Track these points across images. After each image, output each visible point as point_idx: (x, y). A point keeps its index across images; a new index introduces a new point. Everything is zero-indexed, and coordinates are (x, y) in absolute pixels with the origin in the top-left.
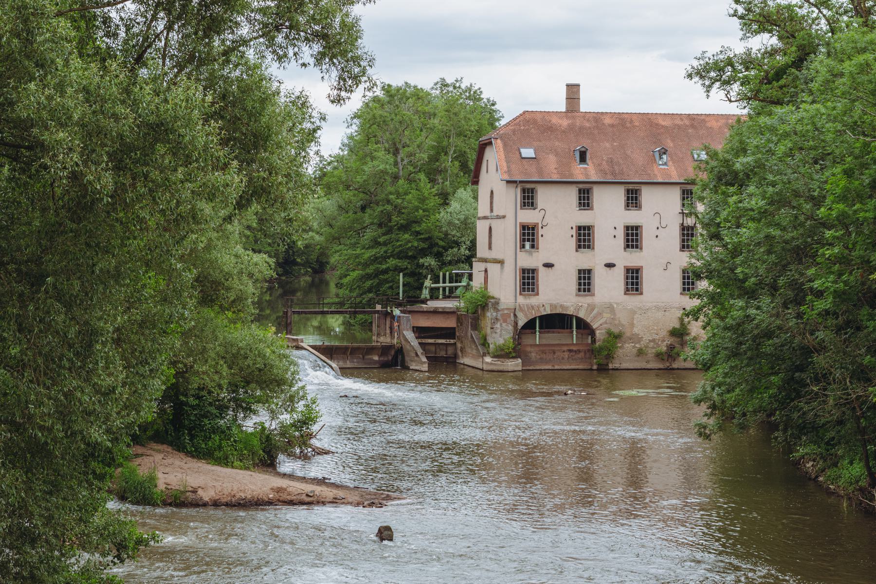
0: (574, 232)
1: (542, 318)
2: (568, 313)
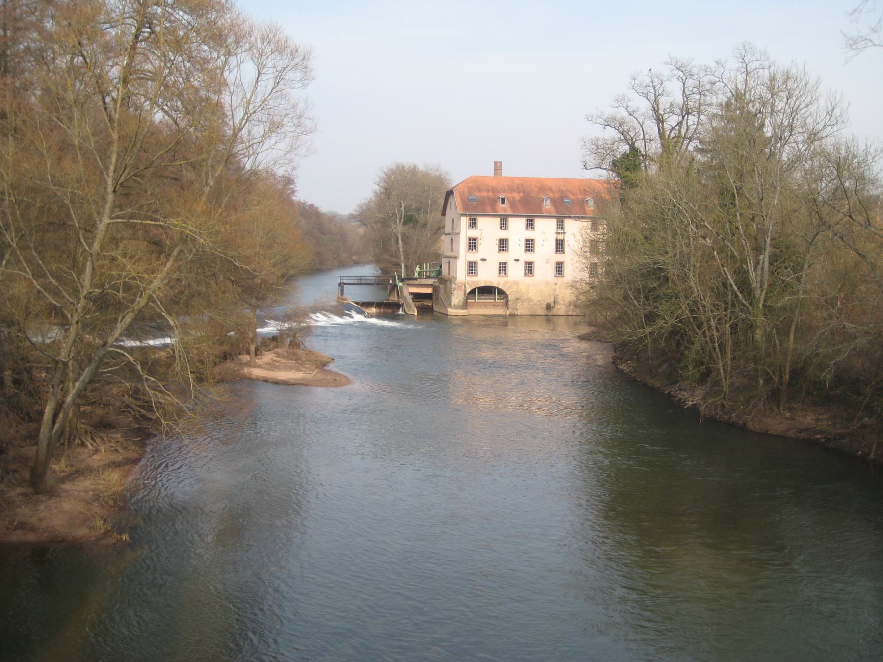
0: (498, 242)
1: (479, 288)
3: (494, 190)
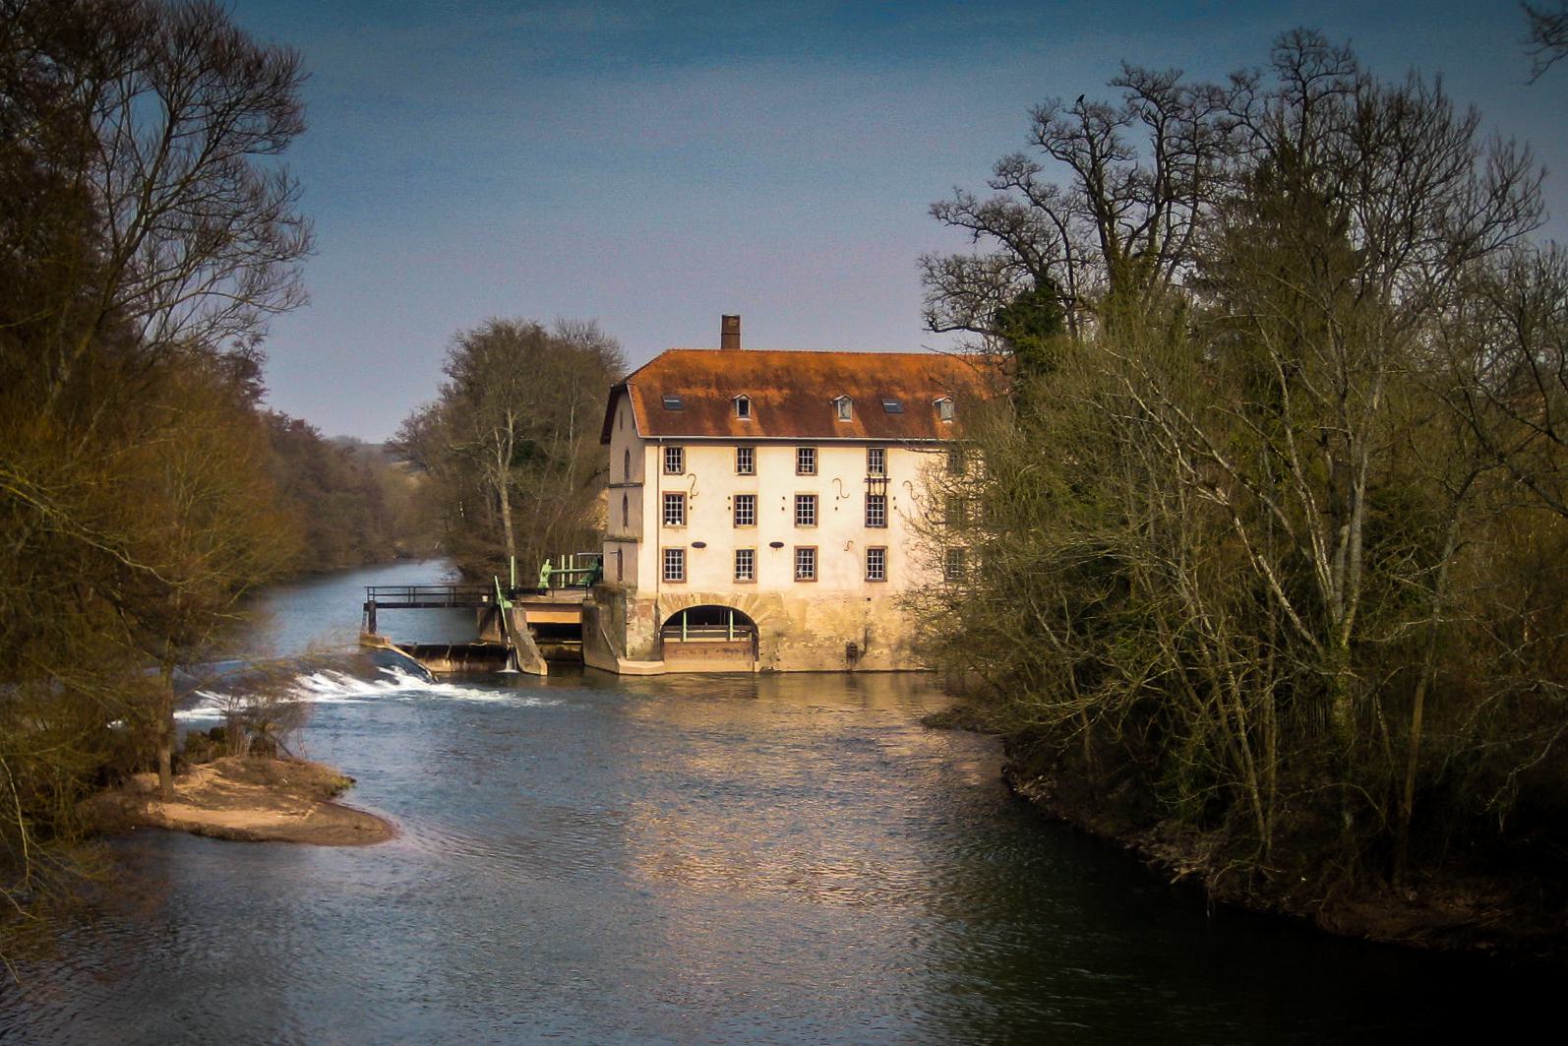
0: (731, 503)
1: (689, 611)
2: (724, 605)
3: (722, 382)
